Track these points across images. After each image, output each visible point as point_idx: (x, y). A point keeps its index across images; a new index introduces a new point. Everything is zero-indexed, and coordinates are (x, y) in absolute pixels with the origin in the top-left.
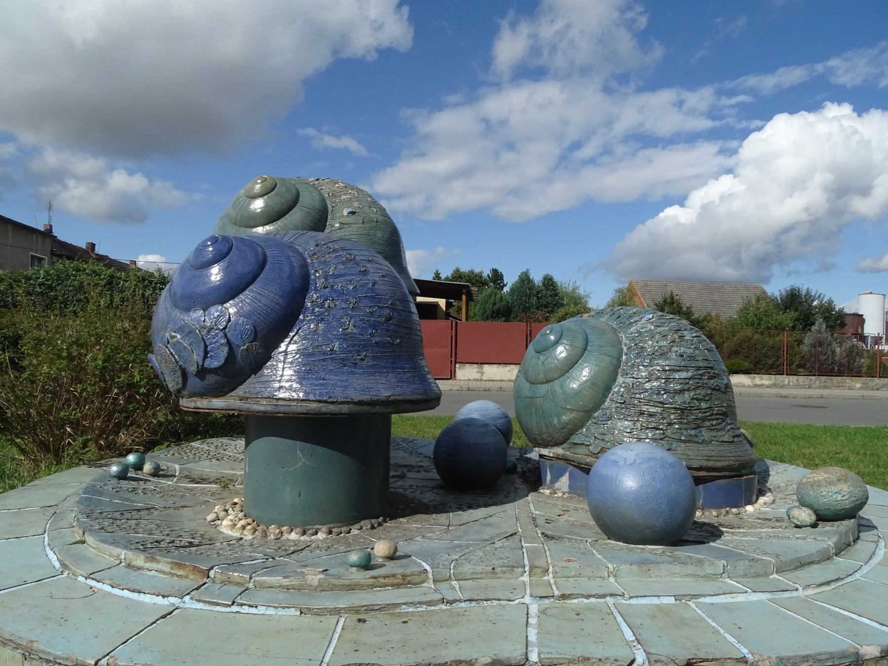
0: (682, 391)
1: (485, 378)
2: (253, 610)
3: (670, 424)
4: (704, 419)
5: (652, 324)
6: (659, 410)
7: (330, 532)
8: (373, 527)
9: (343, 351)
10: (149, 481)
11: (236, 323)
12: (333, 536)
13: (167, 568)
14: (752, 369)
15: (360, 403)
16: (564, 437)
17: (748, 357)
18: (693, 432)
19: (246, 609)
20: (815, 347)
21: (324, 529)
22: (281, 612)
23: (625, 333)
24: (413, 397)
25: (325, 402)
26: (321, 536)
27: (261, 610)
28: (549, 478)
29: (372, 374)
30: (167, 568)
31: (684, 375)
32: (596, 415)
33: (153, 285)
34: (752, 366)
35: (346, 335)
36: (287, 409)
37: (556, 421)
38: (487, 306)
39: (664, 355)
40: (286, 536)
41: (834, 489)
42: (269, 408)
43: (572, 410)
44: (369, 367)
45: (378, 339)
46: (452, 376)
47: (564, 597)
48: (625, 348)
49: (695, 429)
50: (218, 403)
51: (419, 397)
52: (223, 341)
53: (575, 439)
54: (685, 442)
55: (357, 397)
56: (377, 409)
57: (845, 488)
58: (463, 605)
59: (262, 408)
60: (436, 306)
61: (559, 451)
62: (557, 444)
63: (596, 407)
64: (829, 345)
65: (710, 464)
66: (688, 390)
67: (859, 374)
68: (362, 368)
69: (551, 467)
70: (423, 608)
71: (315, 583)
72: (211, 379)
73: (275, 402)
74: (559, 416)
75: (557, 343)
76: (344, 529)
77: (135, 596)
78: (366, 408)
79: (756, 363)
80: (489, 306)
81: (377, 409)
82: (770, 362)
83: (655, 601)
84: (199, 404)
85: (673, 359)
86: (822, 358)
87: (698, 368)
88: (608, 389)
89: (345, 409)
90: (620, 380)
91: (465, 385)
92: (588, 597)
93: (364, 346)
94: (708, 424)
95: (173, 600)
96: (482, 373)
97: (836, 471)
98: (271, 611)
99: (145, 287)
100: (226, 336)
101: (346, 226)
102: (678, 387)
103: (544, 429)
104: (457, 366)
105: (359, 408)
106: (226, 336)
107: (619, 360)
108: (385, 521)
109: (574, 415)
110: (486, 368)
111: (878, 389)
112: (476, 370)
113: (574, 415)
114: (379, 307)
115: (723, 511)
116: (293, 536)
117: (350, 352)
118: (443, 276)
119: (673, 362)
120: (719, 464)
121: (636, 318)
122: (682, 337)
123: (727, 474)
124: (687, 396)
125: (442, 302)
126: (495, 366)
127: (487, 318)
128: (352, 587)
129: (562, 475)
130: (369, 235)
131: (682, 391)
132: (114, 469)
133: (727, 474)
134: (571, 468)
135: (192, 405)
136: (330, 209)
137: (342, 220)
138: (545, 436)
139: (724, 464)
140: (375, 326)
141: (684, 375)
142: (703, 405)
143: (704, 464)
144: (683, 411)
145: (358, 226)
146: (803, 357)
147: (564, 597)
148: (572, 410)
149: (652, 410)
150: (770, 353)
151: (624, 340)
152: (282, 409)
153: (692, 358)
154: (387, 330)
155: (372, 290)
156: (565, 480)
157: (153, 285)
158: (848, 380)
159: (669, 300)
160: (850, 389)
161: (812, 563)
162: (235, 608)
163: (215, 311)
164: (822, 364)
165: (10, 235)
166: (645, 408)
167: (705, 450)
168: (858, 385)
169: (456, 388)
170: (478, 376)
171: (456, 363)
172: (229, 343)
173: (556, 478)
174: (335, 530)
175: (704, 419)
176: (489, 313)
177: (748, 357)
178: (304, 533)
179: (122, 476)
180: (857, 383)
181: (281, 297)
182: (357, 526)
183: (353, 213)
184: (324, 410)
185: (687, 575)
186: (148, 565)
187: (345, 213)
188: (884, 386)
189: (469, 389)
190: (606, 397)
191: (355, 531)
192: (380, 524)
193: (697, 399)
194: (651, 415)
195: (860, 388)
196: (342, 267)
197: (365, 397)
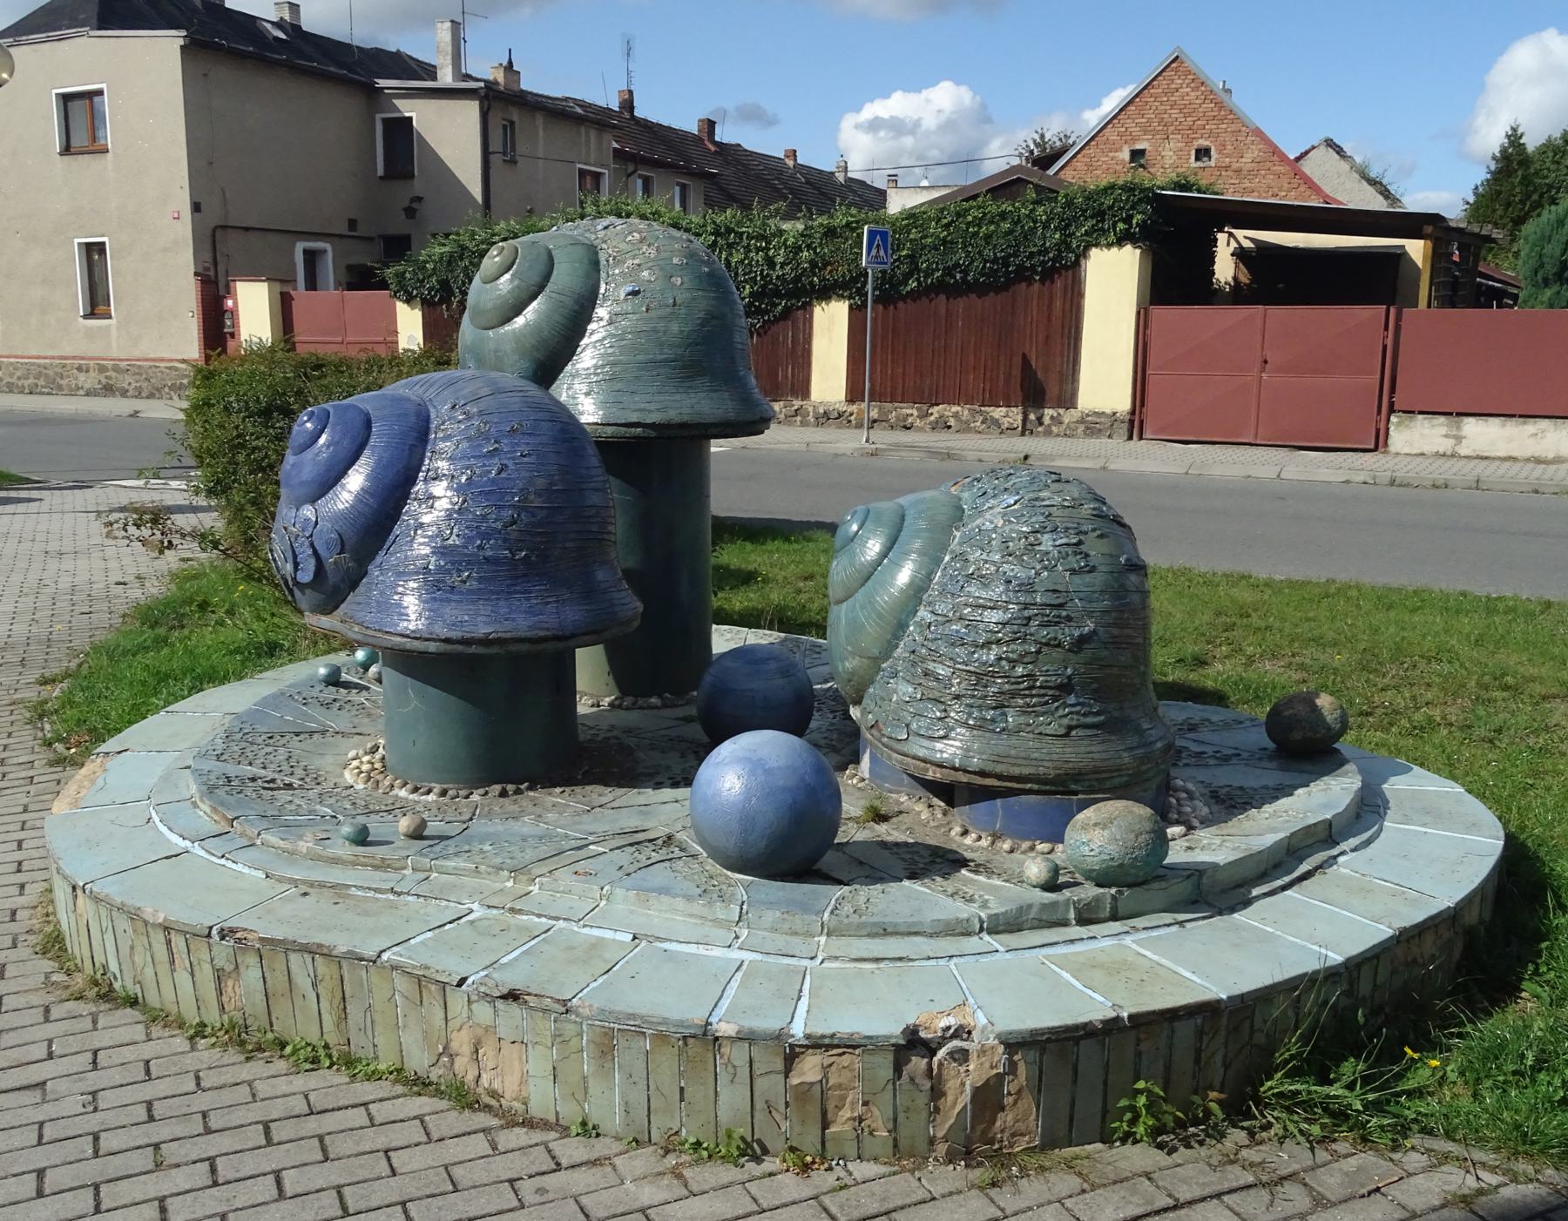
1: (1463, 451)
2: (234, 866)
7: (444, 793)
8: (504, 794)
9: (439, 569)
10: (367, 688)
12: (445, 800)
15: (447, 641)
18: (989, 714)
19: (229, 864)
21: (437, 788)
24: (529, 634)
26: (431, 797)
27: (239, 867)
29: (474, 602)
33: (745, 242)
35: (444, 547)
38: (1548, 249)
40: (396, 791)
44: (470, 592)
45: (489, 553)
46: (1379, 442)
49: (994, 708)
51: (542, 633)
52: (310, 552)
54: (972, 728)
55: (444, 632)
56: (473, 649)
58: (410, 898)
60: (1397, 258)
65: (999, 769)
66: (998, 642)
68: (461, 593)
70: (371, 894)
74: (843, 660)
76: (463, 793)
78: (460, 648)
80: (1553, 249)
81: (473, 649)
89: (432, 647)
91: (1403, 470)
92: (539, 916)
93: (469, 562)
94: (1020, 702)
95: (187, 843)
96: (1459, 439)
98: (246, 870)
99: (730, 246)
100: (312, 545)
101: (620, 318)
104: (1394, 419)
105: (449, 647)
106: (312, 545)
108: (530, 788)
110: (1471, 426)
112: (1444, 430)
114: (499, 507)
115: (1026, 845)
116: (403, 793)
117: (449, 572)
118: (1532, 142)
120: (1016, 771)
123: (1036, 787)
125: (1416, 249)
126: (1497, 420)
127: (1546, 282)
128: (335, 861)
130: (655, 331)
132: (323, 671)
133: (1036, 787)
139: (1026, 771)
140: (485, 536)
143: (989, 767)
153: (1028, 587)
154: (505, 540)
155: (493, 481)
157: (745, 242)
161: (897, 933)
162: (223, 861)
163: (308, 512)
165: (541, 132)
167: (1002, 744)
169: (1361, 477)
170: (1445, 445)
171: (1392, 410)
172: (316, 553)
174: (451, 793)
176: (1550, 269)
178: (415, 790)
179: (334, 680)
181: (371, 495)
182: (482, 791)
183: (635, 293)
184: (408, 646)
185: (691, 916)
187: (622, 296)
189: (1392, 483)
191: (475, 797)
192: (518, 792)
193: (1009, 661)
196: (464, 445)
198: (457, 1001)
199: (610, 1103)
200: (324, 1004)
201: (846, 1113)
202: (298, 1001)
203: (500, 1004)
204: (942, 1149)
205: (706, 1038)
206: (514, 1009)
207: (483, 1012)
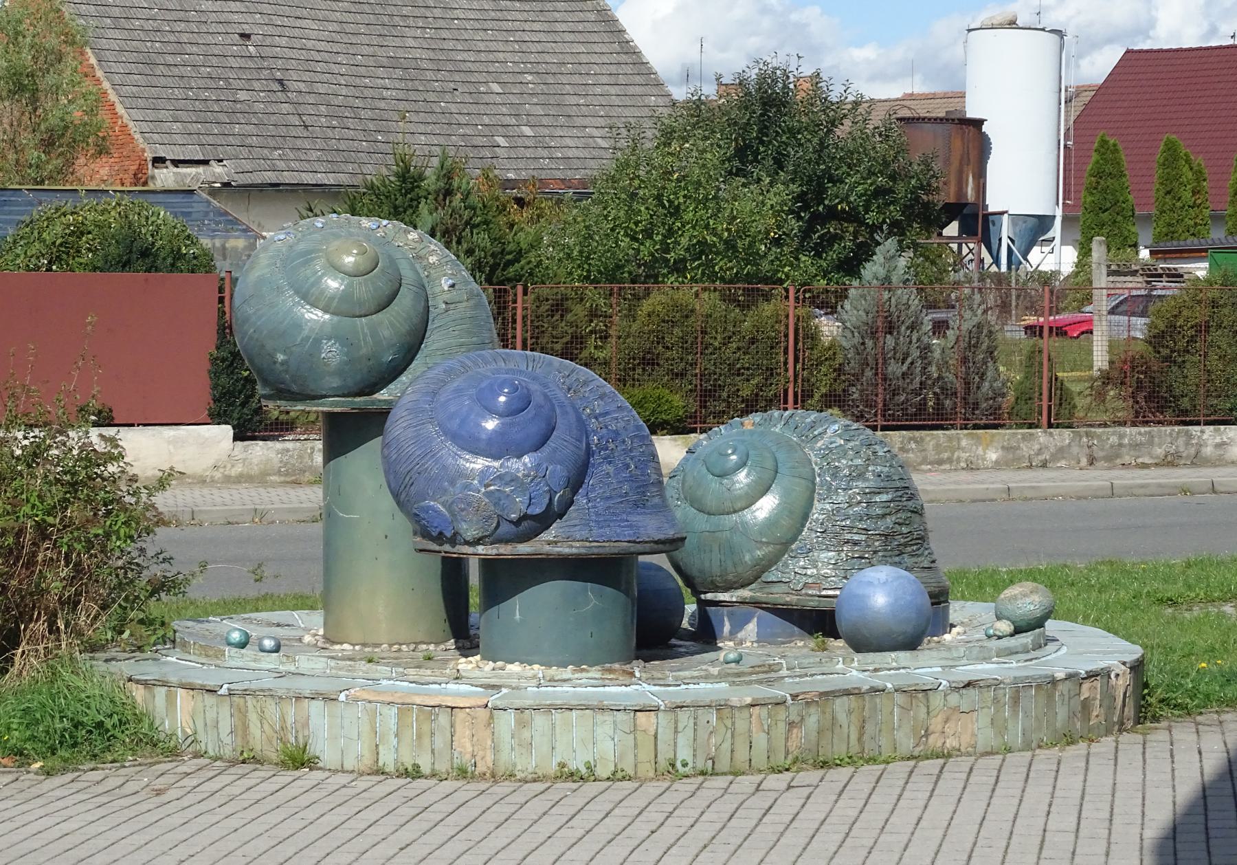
0: (884, 516)
3: (875, 552)
4: (906, 545)
5: (840, 436)
6: (864, 537)
11: (554, 471)
13: (598, 675)
14: (693, 416)
16: (756, 575)
17: (681, 375)
19: (691, 686)
20: (873, 334)
22: (717, 686)
23: (812, 449)
25: (634, 542)
28: (727, 628)
30: (598, 675)
31: (885, 497)
32: (793, 547)
34: (694, 406)
36: (601, 551)
37: (747, 558)
39: (861, 476)
41: (1028, 600)
42: (583, 551)
43: (768, 543)
47: (876, 670)
48: (816, 469)
50: (524, 549)
53: (771, 576)
57: (1036, 598)
59: (574, 551)
61: (745, 593)
62: (743, 586)
63: (794, 539)
64: (912, 327)
67: (990, 418)
69: (731, 616)
70: (797, 680)
71: (716, 673)
72: (525, 524)
73: (588, 544)
75: (742, 465)
77: (601, 689)
79: (706, 396)
82: (746, 392)
83: (929, 670)
84: (502, 551)
85: (871, 481)
86: (895, 369)
87: (897, 489)
88: (805, 517)
90: (817, 505)
94: (909, 549)
97: (1029, 585)
98: (709, 686)
102: (879, 511)
103: (730, 568)
107: (814, 484)
109: (771, 548)
111: (1044, 465)
113: (771, 548)
119: (871, 484)
121: (820, 430)
122: (875, 453)
124: (889, 521)
129: (747, 622)
131: (884, 516)
134: (760, 611)
135: (495, 552)
136: (425, 281)
137: (446, 297)
138: (730, 577)
141: (885, 497)
142: (904, 530)
144: (887, 536)
145: (464, 304)
146: (839, 370)
147: (876, 670)
148: (768, 543)
149: (856, 537)
150: (746, 360)
151: (813, 459)
152: (596, 551)
153: (889, 477)
156: (752, 627)
158: (965, 441)
159: (431, 181)
160: (971, 467)
164: (895, 393)
166: (848, 536)
168: (993, 456)
173: (738, 625)
175: (906, 545)
177: (681, 375)
180: (988, 448)
183: (453, 286)
186: (576, 676)
188: (1061, 452)
190: (803, 526)
194: (856, 543)
195: (997, 465)
197: (662, 537)
198: (936, 700)
199: (1015, 734)
200: (853, 728)
201: (1095, 713)
202: (837, 730)
203: (964, 691)
204: (1116, 728)
205: (1054, 682)
206: (971, 692)
207: (954, 699)
